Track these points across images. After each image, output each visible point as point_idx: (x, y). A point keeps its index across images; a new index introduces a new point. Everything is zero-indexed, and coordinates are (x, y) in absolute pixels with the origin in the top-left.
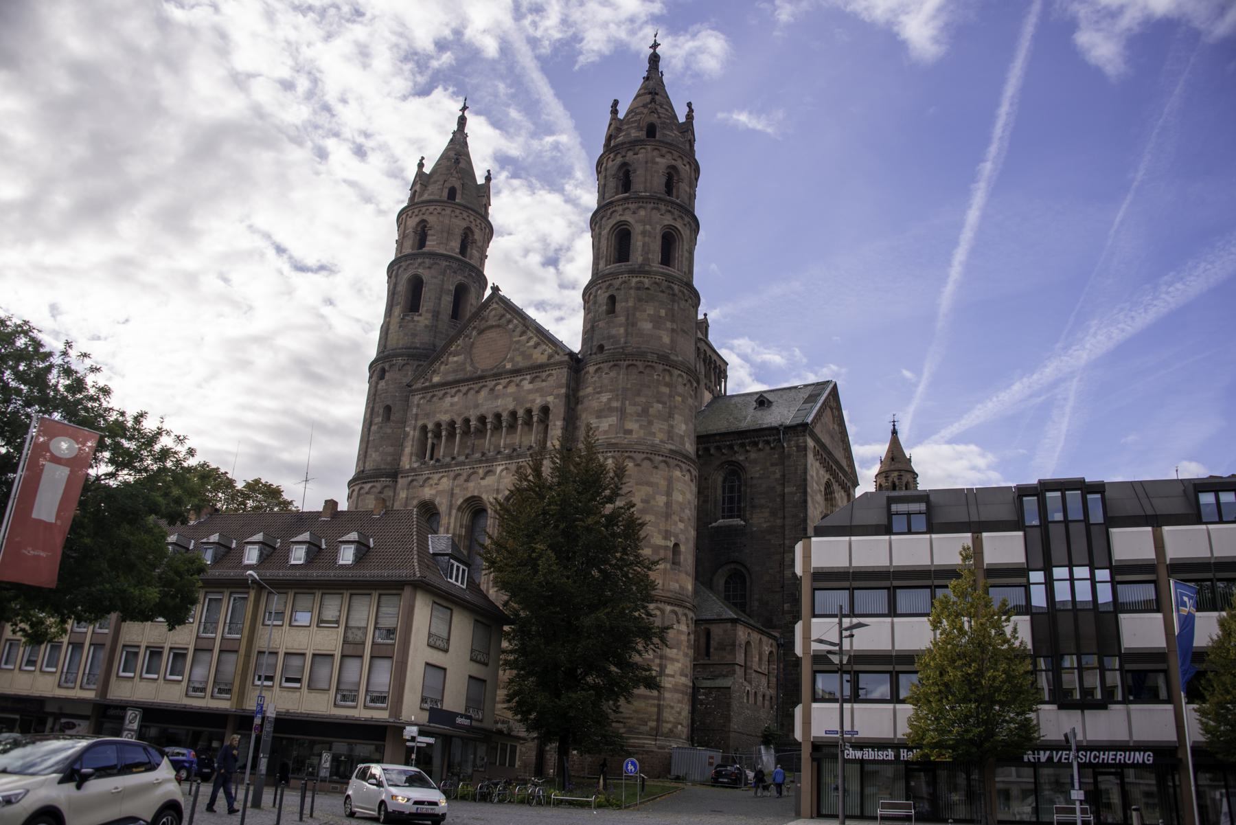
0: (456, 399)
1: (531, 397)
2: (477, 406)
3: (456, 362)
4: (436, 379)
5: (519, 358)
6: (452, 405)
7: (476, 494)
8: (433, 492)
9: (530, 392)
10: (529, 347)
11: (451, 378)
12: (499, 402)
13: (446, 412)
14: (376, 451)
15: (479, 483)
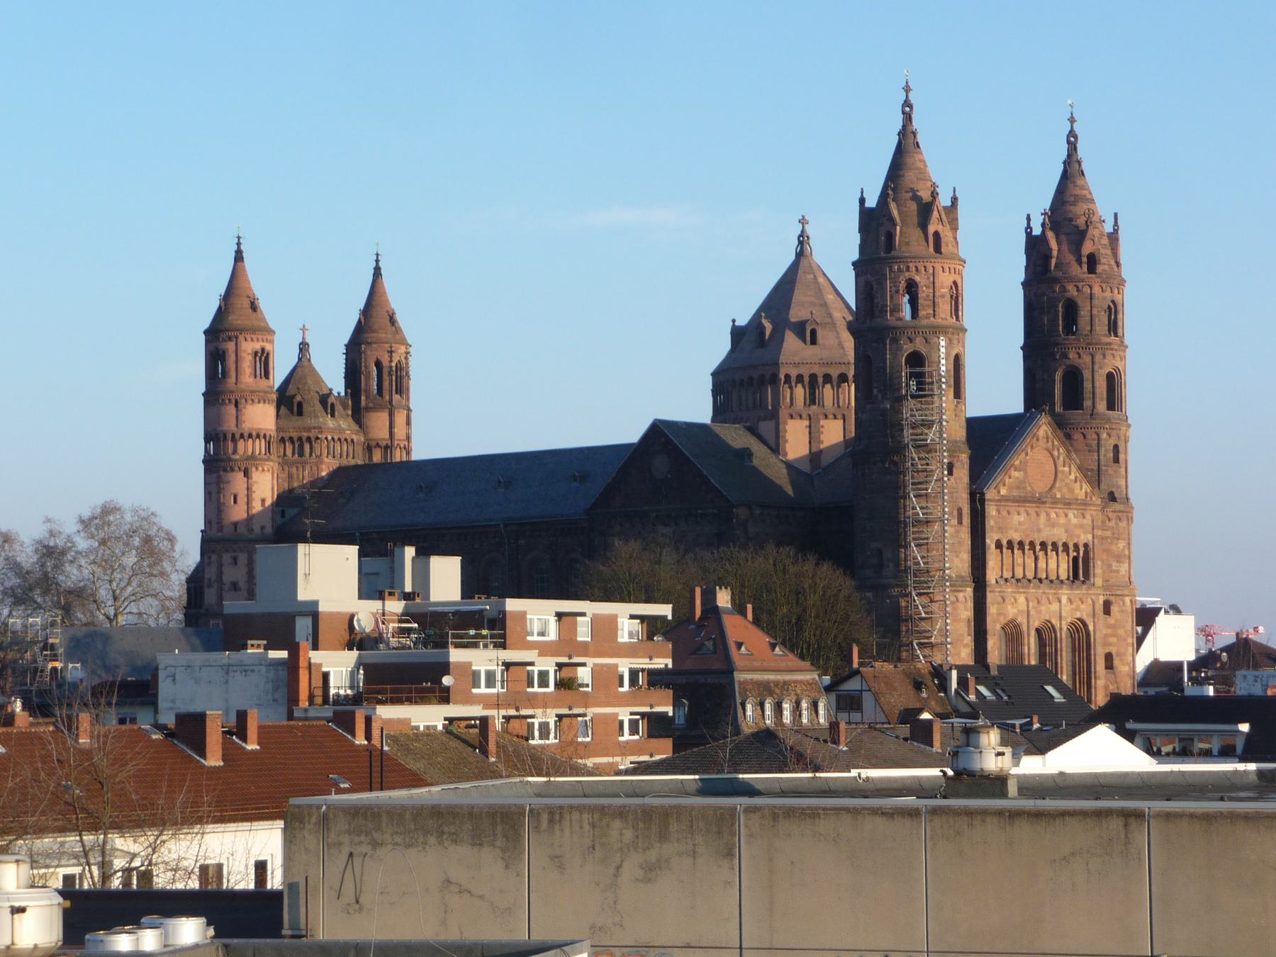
0: (1022, 518)
1: (1077, 532)
2: (1039, 530)
3: (1018, 478)
4: (1003, 492)
5: (1065, 490)
6: (1020, 523)
7: (1047, 618)
8: (1015, 611)
9: (1076, 526)
10: (1071, 480)
11: (1015, 493)
12: (1055, 531)
13: (1016, 531)
14: (957, 557)
15: (1049, 608)
